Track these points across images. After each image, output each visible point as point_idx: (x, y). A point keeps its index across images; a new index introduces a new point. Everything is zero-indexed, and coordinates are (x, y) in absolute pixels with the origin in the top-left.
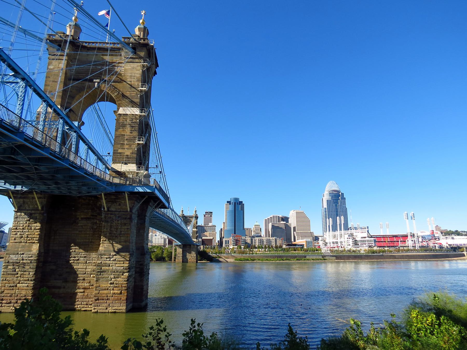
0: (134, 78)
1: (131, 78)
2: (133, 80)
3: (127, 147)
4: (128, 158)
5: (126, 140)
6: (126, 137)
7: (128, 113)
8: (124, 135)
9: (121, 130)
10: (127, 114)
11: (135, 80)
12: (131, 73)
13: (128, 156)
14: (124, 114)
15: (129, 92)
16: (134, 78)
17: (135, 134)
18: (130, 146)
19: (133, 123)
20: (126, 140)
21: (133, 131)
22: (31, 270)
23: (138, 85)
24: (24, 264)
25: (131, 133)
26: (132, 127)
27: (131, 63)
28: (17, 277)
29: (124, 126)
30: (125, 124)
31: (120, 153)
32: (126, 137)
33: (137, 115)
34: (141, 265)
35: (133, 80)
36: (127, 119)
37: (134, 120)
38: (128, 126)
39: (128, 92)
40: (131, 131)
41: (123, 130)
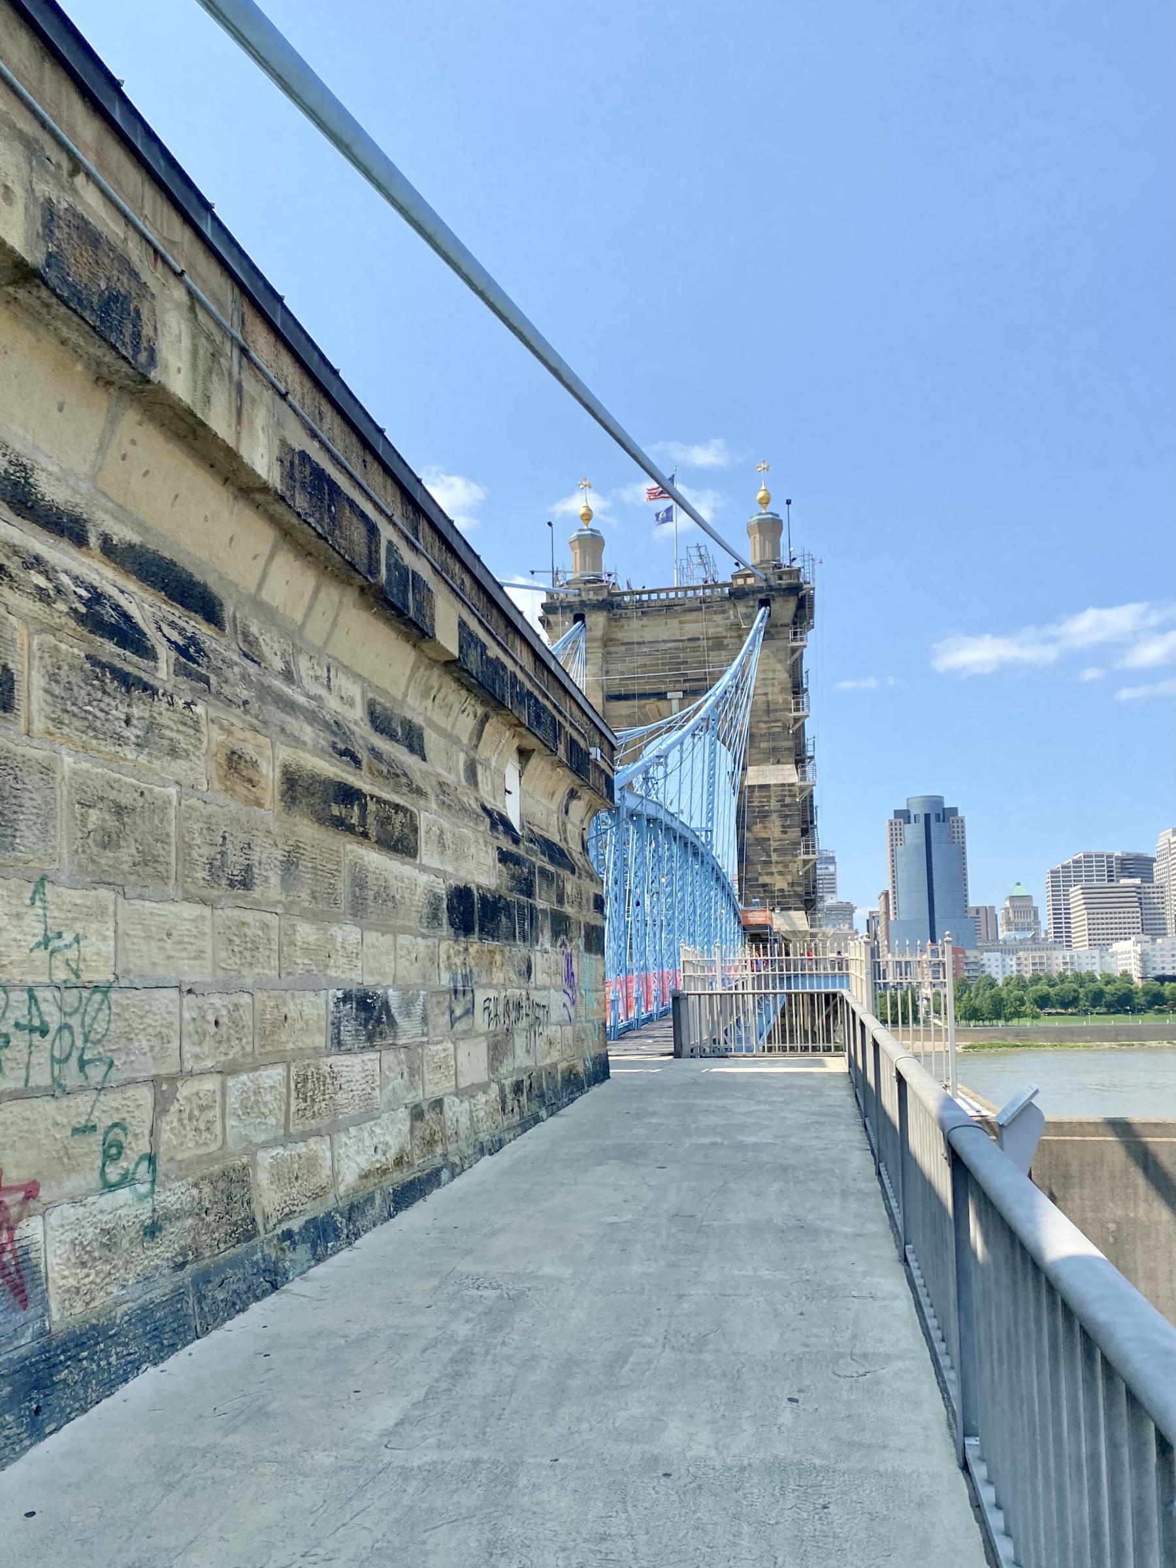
0: (773, 685)
2: (770, 690)
3: (780, 868)
4: (783, 896)
5: (775, 850)
6: (774, 845)
8: (769, 839)
9: (759, 825)
10: (769, 786)
11: (777, 689)
13: (782, 890)
14: (762, 787)
15: (765, 722)
16: (773, 685)
18: (786, 866)
19: (786, 806)
20: (775, 850)
21: (789, 826)
23: (786, 702)
25: (785, 832)
26: (787, 816)
29: (764, 815)
30: (767, 811)
31: (764, 885)
32: (774, 845)
33: (792, 785)
35: (770, 690)
37: (788, 800)
38: (774, 816)
39: (762, 725)
40: (783, 826)
41: (765, 827)
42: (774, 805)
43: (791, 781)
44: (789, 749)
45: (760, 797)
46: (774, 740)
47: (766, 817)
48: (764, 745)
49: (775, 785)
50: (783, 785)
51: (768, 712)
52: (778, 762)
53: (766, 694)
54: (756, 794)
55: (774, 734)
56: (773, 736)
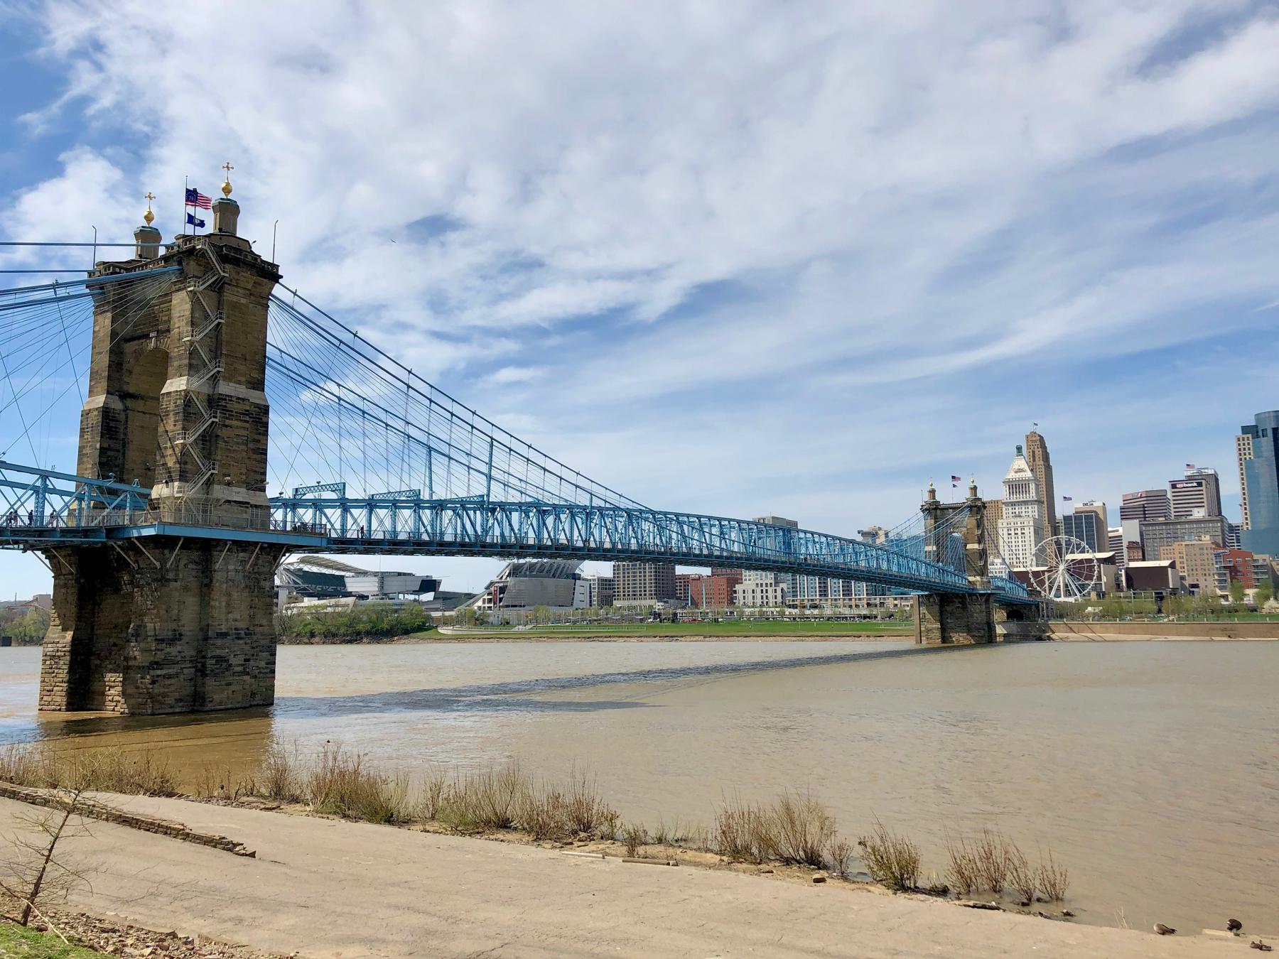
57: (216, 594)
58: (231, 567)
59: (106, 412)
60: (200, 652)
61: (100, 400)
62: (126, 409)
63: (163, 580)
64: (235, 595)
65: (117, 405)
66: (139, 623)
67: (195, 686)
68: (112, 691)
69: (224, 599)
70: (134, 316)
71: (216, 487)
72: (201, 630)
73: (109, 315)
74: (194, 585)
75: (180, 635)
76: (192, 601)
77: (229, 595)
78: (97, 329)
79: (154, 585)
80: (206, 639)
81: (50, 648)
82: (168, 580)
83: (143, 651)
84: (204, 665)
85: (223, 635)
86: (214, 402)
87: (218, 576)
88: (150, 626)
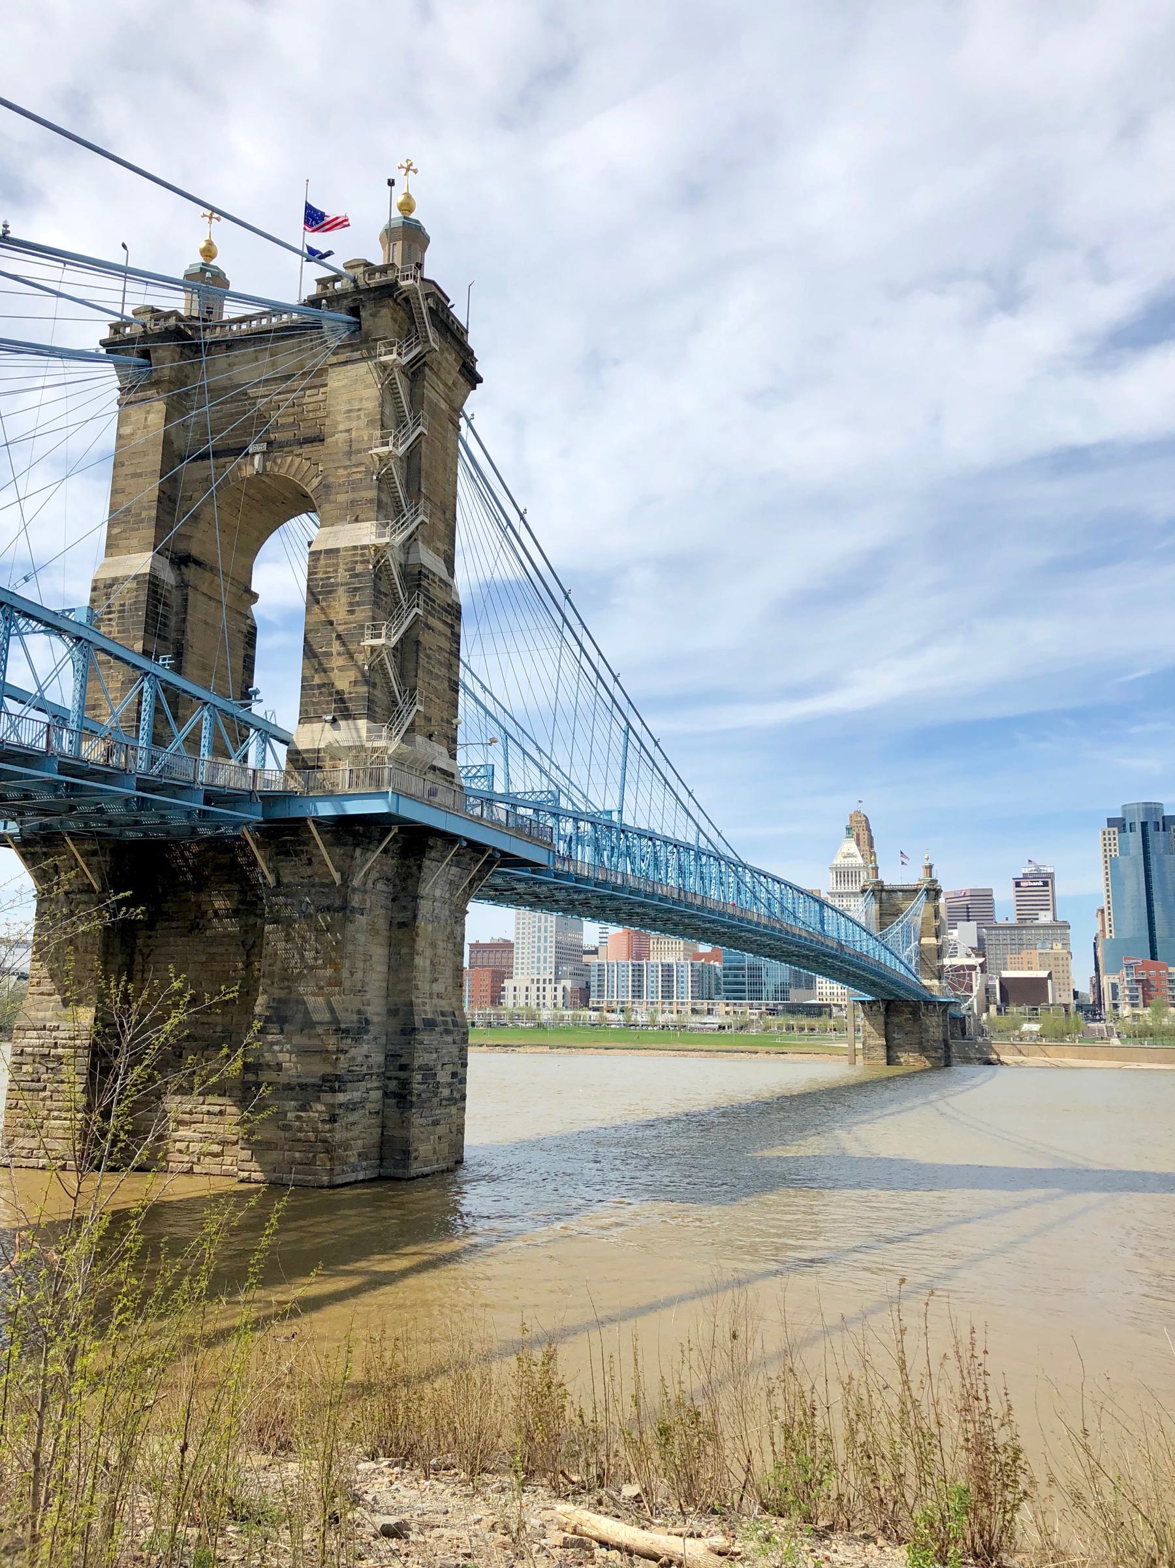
0: (359, 417)
1: (349, 419)
2: (354, 424)
7: (341, 543)
10: (337, 550)
11: (363, 422)
12: (349, 402)
14: (329, 552)
15: (345, 468)
16: (359, 417)
17: (363, 613)
19: (357, 576)
21: (358, 604)
22: (78, 1079)
24: (59, 1058)
25: (352, 612)
26: (356, 589)
27: (349, 367)
28: (43, 1099)
29: (329, 590)
30: (332, 585)
34: (403, 1068)
35: (354, 424)
36: (338, 564)
37: (359, 568)
39: (341, 472)
40: (351, 604)
42: (342, 575)
43: (366, 542)
44: (371, 501)
45: (327, 566)
46: (354, 490)
47: (330, 592)
48: (342, 498)
49: (346, 549)
50: (355, 548)
51: (350, 454)
52: (357, 520)
53: (348, 431)
54: (322, 562)
55: (354, 482)
56: (354, 486)
57: (421, 944)
58: (438, 893)
59: (153, 583)
60: (391, 1057)
61: (141, 562)
62: (183, 585)
63: (344, 909)
64: (441, 944)
65: (168, 576)
66: (277, 993)
67: (383, 1127)
68: (183, 1132)
69: (428, 953)
70: (204, 411)
71: (419, 739)
72: (392, 1012)
73: (159, 407)
74: (382, 924)
75: (367, 1022)
76: (379, 952)
77: (433, 945)
78: (127, 430)
79: (322, 920)
80: (409, 1032)
81: (31, 1040)
82: (353, 910)
83: (303, 1052)
84: (405, 1084)
85: (430, 1024)
86: (416, 578)
87: (425, 907)
88: (315, 1002)
